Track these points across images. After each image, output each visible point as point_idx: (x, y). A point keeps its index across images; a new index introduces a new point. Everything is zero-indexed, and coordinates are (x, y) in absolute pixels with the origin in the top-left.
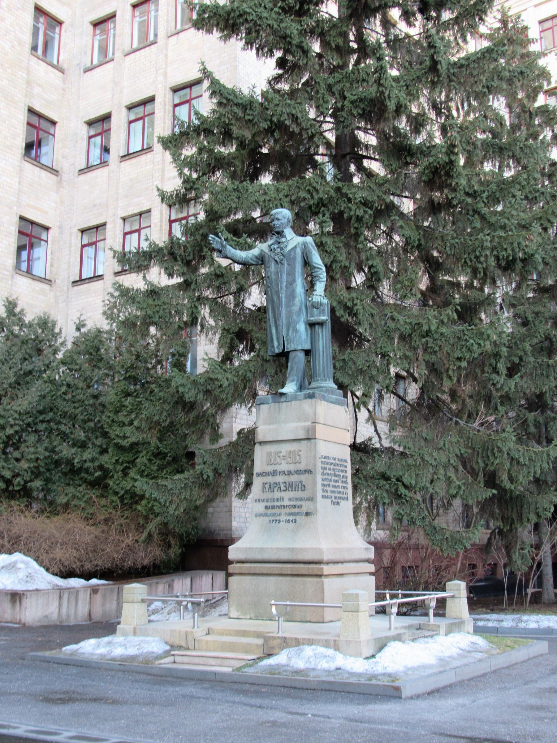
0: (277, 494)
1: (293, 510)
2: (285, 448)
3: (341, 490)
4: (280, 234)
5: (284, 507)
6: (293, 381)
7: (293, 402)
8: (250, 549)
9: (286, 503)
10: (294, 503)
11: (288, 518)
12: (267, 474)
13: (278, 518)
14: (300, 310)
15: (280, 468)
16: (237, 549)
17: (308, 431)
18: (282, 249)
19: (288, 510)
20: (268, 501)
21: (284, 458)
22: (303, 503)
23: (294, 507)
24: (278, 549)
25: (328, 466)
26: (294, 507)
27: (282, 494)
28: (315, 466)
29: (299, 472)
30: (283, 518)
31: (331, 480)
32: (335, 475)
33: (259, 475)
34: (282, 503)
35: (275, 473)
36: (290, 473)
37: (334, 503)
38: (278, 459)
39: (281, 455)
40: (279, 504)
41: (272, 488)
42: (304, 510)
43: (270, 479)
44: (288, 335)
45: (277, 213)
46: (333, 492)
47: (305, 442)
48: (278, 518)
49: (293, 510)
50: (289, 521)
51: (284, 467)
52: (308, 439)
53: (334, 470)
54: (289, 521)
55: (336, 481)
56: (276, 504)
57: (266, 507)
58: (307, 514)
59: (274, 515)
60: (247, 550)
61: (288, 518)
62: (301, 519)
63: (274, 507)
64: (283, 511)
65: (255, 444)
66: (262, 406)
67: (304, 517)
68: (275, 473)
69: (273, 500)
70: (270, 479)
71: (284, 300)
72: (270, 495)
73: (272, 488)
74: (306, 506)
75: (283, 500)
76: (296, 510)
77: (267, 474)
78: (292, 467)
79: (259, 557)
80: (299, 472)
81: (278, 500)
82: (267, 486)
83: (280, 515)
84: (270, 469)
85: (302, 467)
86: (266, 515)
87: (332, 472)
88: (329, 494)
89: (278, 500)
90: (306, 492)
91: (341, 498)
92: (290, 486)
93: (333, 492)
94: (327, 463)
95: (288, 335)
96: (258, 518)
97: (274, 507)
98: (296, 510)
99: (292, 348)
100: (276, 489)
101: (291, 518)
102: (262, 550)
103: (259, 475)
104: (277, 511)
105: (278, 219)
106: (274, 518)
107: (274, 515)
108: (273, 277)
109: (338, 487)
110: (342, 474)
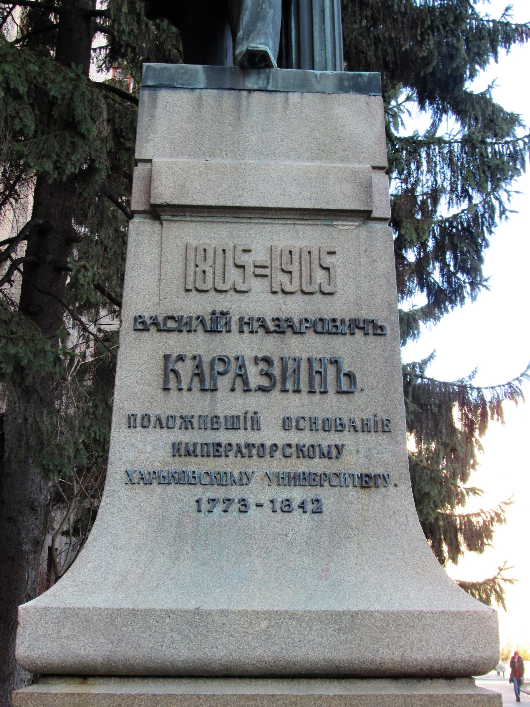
0: (229, 402)
2: (263, 240)
5: (262, 450)
7: (294, 97)
9: (270, 434)
10: (306, 438)
15: (237, 307)
16: (67, 614)
19: (278, 465)
20: (187, 423)
21: (261, 272)
22: (346, 439)
23: (302, 452)
24: (276, 617)
26: (302, 452)
27: (254, 402)
29: (328, 327)
30: (258, 492)
33: (142, 325)
34: (255, 438)
35: (215, 324)
36: (283, 327)
40: (239, 437)
47: (350, 226)
48: (235, 493)
49: (302, 466)
50: (287, 506)
54: (287, 506)
56: (224, 436)
57: (177, 450)
58: (368, 481)
59: (218, 479)
61: (282, 493)
63: (217, 450)
64: (257, 466)
66: (164, 94)
67: (352, 493)
68: (215, 324)
70: (199, 344)
72: (197, 404)
74: (360, 453)
75: (254, 423)
76: (318, 465)
78: (294, 308)
79: (182, 651)
80: (328, 327)
81: (233, 423)
82: (185, 369)
83: (245, 479)
85: (339, 308)
89: (233, 423)
90: (358, 399)
96: (141, 491)
97: (217, 450)
98: (318, 465)
100: (223, 383)
101: (297, 494)
103: (142, 325)
104: (230, 465)
106: (219, 493)
107: (218, 479)
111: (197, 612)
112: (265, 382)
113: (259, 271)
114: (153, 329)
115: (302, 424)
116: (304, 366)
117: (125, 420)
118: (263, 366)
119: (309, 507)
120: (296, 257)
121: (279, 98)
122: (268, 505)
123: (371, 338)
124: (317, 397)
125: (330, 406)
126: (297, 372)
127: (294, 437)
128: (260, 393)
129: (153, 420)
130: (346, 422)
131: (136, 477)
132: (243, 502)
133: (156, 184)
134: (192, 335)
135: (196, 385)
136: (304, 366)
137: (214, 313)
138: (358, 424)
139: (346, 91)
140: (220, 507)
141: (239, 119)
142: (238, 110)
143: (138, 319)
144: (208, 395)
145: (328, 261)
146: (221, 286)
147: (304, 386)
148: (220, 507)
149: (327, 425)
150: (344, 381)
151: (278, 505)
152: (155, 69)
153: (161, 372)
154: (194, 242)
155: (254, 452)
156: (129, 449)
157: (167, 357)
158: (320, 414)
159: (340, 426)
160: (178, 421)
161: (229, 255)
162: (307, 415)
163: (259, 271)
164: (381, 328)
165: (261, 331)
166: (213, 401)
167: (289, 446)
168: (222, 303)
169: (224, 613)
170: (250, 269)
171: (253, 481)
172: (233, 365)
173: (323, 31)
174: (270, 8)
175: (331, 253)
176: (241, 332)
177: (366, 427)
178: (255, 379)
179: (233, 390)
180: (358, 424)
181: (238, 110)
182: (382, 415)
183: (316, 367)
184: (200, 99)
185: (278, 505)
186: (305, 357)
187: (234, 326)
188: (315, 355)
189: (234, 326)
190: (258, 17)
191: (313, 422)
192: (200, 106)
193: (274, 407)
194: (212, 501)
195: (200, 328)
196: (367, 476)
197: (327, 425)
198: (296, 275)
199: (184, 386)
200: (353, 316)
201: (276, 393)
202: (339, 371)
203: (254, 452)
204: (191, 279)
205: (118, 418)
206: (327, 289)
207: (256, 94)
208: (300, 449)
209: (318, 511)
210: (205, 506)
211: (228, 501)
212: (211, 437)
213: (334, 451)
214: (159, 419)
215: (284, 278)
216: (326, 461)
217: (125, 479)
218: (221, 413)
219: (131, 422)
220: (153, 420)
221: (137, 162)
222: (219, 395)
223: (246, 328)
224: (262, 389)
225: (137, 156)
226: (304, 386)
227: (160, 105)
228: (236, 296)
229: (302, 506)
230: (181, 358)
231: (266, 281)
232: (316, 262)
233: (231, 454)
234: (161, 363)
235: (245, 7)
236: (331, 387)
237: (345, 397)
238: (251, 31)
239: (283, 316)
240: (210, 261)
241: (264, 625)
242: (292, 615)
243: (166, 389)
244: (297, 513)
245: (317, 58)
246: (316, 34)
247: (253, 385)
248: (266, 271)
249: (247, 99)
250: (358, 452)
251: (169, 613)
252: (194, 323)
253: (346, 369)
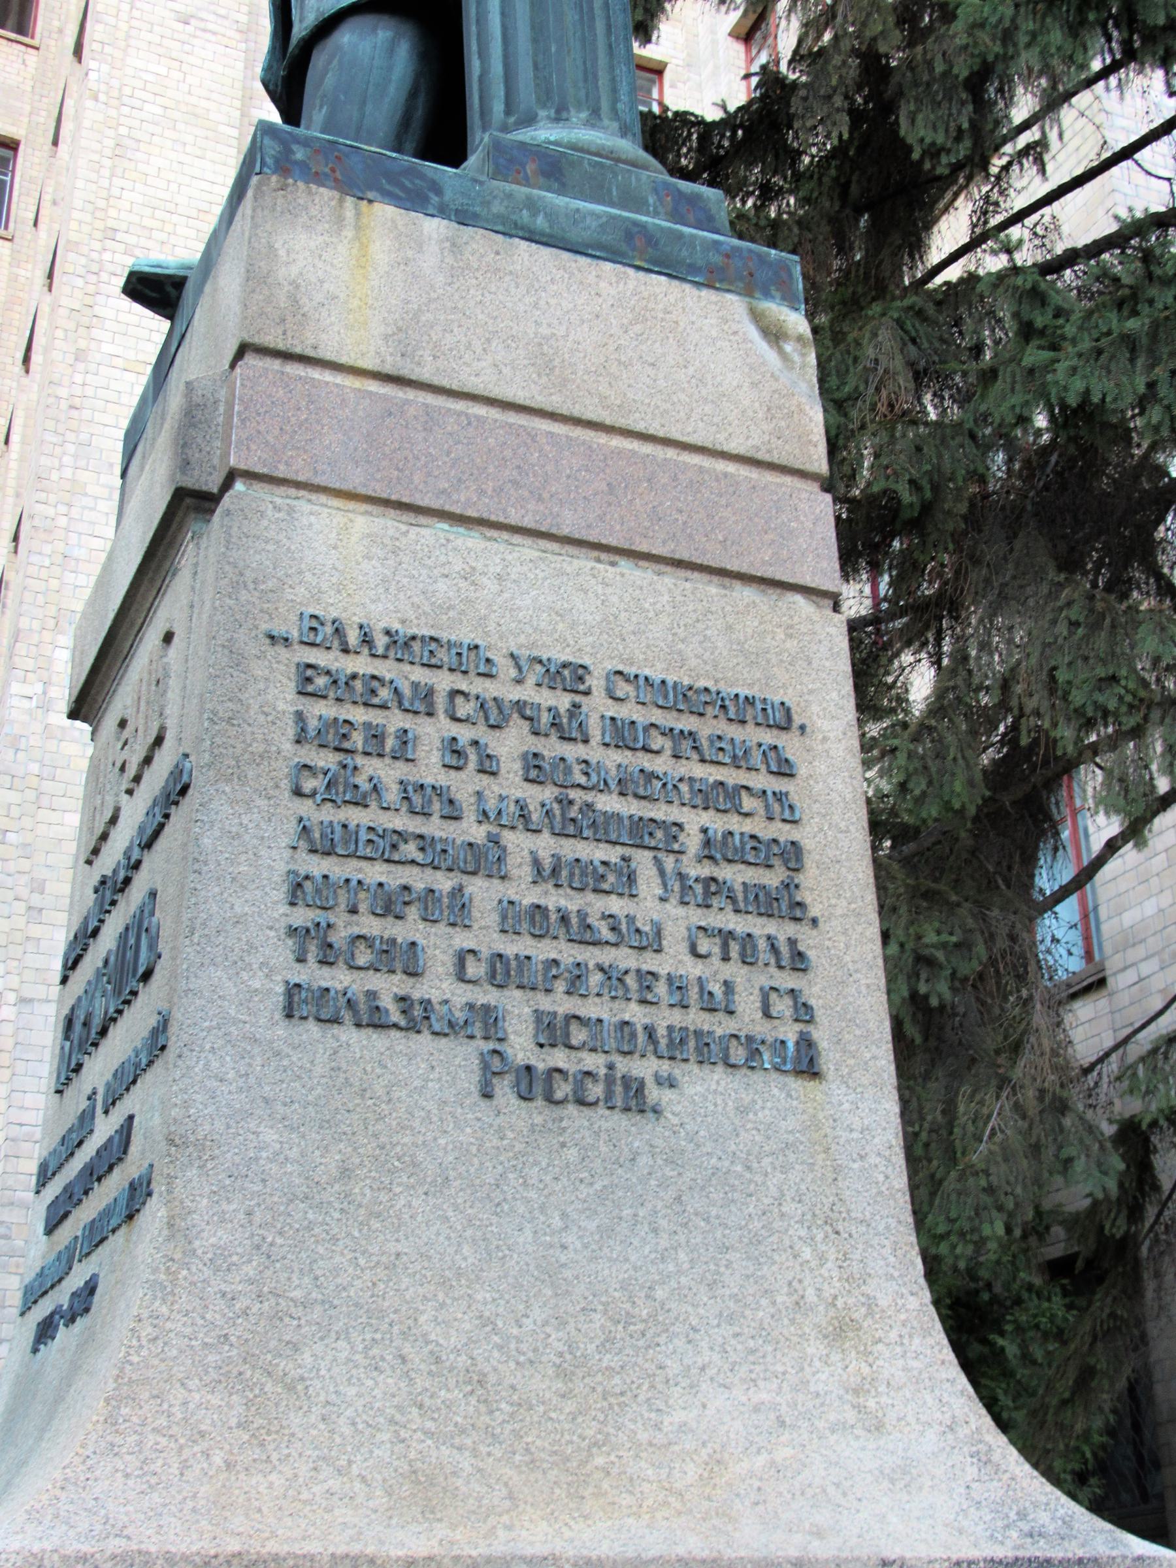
3: (673, 960)
25: (431, 733)
31: (485, 860)
32: (569, 825)
37: (532, 1084)
46: (502, 971)
53: (535, 769)
55: (591, 879)
87: (511, 784)
88: (438, 986)
91: (707, 1051)
93: (502, 971)
94: (423, 702)
109: (653, 942)
110: (694, 821)
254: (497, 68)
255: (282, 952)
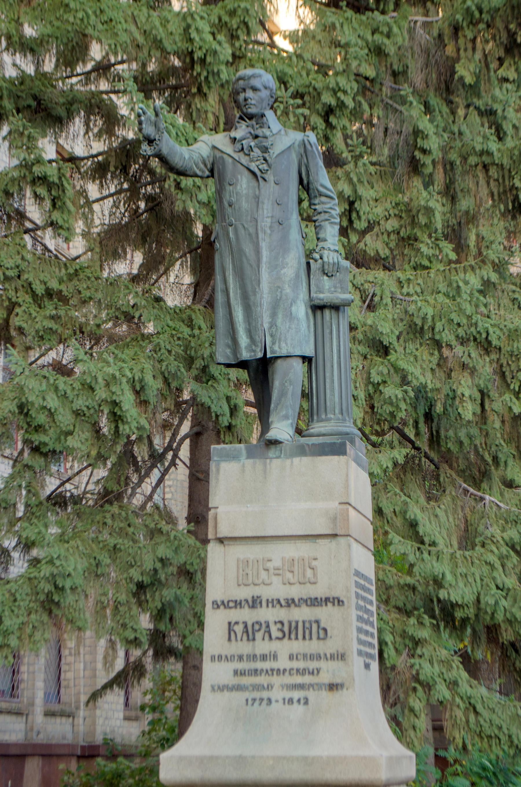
0: (262, 646)
1: (299, 680)
4: (257, 118)
6: (286, 417)
7: (296, 460)
8: (212, 759)
9: (283, 663)
10: (301, 664)
11: (288, 695)
12: (238, 604)
13: (265, 694)
14: (297, 276)
15: (266, 593)
16: (181, 759)
17: (334, 520)
18: (265, 150)
20: (240, 658)
21: (278, 572)
22: (323, 664)
23: (301, 672)
24: (278, 759)
26: (301, 672)
28: (348, 590)
29: (314, 602)
30: (277, 694)
33: (216, 605)
34: (275, 665)
35: (255, 603)
36: (290, 603)
38: (264, 575)
39: (270, 565)
41: (250, 632)
42: (325, 678)
43: (245, 615)
44: (273, 324)
45: (254, 76)
48: (265, 694)
49: (299, 680)
50: (291, 701)
51: (277, 590)
52: (335, 535)
54: (291, 701)
56: (259, 665)
57: (236, 672)
58: (333, 687)
60: (202, 760)
61: (288, 695)
62: (320, 698)
63: (256, 672)
64: (276, 680)
65: (205, 541)
67: (324, 693)
68: (255, 603)
69: (253, 657)
70: (245, 615)
71: (265, 254)
73: (250, 632)
74: (329, 671)
75: (275, 657)
76: (307, 679)
77: (238, 604)
80: (314, 602)
81: (264, 658)
82: (239, 629)
83: (270, 687)
84: (244, 593)
85: (319, 591)
86: (239, 688)
89: (264, 658)
92: (290, 631)
95: (273, 324)
96: (219, 695)
97: (256, 672)
98: (307, 679)
99: (284, 352)
100: (259, 636)
101: (296, 695)
102: (240, 760)
103: (216, 605)
105: (255, 89)
106: (257, 695)
108: (245, 205)
111: (241, 757)
112: (280, 635)
113: (277, 572)
114: (222, 607)
115: (299, 657)
116: (300, 625)
117: (209, 659)
118: (279, 626)
119: (302, 701)
120: (296, 563)
121: (288, 462)
122: (281, 701)
123: (336, 607)
124: (307, 642)
125: (314, 646)
126: (297, 628)
127: (295, 664)
128: (277, 641)
129: (223, 658)
130: (322, 656)
131: (216, 688)
132: (269, 700)
133: (219, 525)
134: (242, 610)
135: (245, 637)
136: (300, 625)
137: (253, 597)
138: (328, 656)
139: (326, 455)
140: (257, 703)
141: (265, 478)
142: (265, 471)
143: (214, 603)
144: (251, 643)
145: (314, 563)
146: (256, 582)
147: (300, 636)
148: (257, 703)
149: (313, 657)
150: (321, 632)
151: (286, 701)
152: (218, 449)
153: (227, 632)
154: (242, 557)
155: (275, 673)
156: (213, 673)
157: (230, 623)
158: (308, 651)
159: (319, 657)
160: (236, 658)
161: (261, 563)
162: (302, 652)
163: (277, 572)
164: (343, 602)
165: (278, 606)
166: (254, 647)
167: (291, 669)
168: (257, 591)
169: (253, 757)
170: (272, 571)
171: (274, 688)
172: (264, 626)
173: (333, 381)
174: (290, 385)
175: (315, 559)
176: (268, 606)
177: (332, 657)
178: (275, 633)
179: (263, 639)
180: (328, 656)
181: (265, 471)
182: (341, 651)
183: (307, 625)
184: (243, 466)
185: (286, 701)
186: (301, 620)
187: (264, 604)
188: (306, 618)
189: (264, 604)
190: (283, 394)
191: (305, 656)
192: (243, 471)
193: (285, 648)
194: (254, 700)
195: (246, 606)
196: (333, 685)
197: (313, 657)
198: (296, 573)
199: (239, 638)
200: (327, 595)
201: (286, 640)
202: (319, 627)
203: (275, 673)
204: (240, 578)
205: (206, 657)
206: (312, 580)
207: (274, 461)
208: (298, 670)
209: (306, 702)
210: (250, 702)
211: (262, 700)
212: (253, 665)
213: (316, 672)
214: (226, 657)
215: (289, 575)
216: (311, 677)
217: (210, 688)
218: (258, 652)
219: (213, 658)
220: (223, 658)
221: (210, 509)
222: (257, 642)
223: (270, 605)
224: (278, 638)
225: (210, 505)
226: (300, 636)
227: (222, 472)
228: (265, 587)
229: (299, 701)
230: (237, 623)
231: (280, 578)
232: (307, 565)
233: (263, 674)
234: (227, 626)
235: (274, 386)
236: (314, 636)
237: (321, 642)
238: (278, 404)
239: (290, 597)
240: (250, 567)
241: (271, 762)
242: (284, 758)
243: (229, 639)
244: (296, 704)
245: (328, 404)
246: (328, 386)
247: (273, 636)
248: (280, 572)
249: (270, 464)
250: (328, 671)
251: (227, 757)
252: (243, 603)
253: (322, 625)
254: (337, 399)
255: (355, 641)
